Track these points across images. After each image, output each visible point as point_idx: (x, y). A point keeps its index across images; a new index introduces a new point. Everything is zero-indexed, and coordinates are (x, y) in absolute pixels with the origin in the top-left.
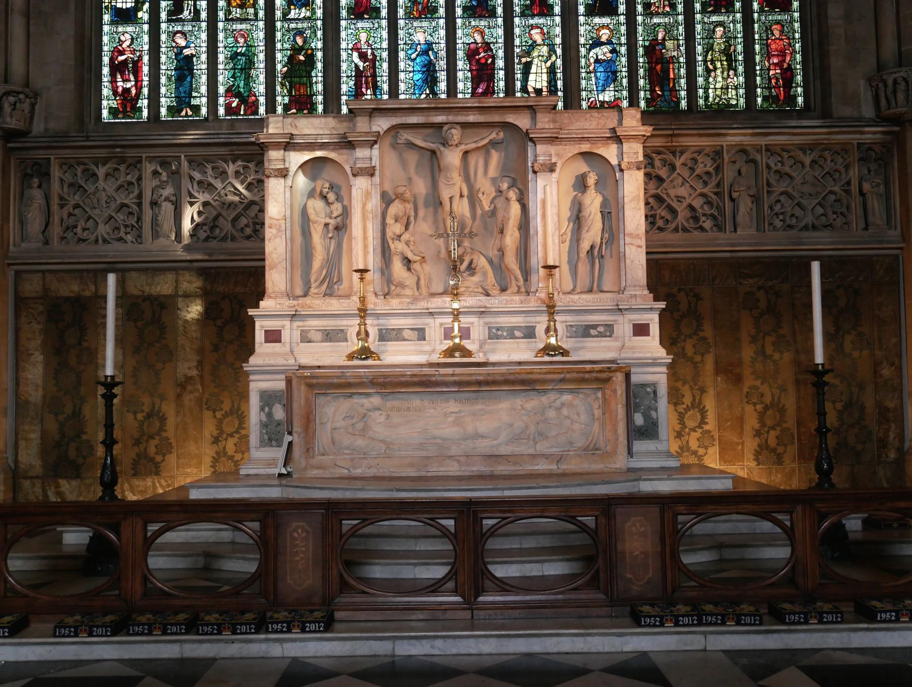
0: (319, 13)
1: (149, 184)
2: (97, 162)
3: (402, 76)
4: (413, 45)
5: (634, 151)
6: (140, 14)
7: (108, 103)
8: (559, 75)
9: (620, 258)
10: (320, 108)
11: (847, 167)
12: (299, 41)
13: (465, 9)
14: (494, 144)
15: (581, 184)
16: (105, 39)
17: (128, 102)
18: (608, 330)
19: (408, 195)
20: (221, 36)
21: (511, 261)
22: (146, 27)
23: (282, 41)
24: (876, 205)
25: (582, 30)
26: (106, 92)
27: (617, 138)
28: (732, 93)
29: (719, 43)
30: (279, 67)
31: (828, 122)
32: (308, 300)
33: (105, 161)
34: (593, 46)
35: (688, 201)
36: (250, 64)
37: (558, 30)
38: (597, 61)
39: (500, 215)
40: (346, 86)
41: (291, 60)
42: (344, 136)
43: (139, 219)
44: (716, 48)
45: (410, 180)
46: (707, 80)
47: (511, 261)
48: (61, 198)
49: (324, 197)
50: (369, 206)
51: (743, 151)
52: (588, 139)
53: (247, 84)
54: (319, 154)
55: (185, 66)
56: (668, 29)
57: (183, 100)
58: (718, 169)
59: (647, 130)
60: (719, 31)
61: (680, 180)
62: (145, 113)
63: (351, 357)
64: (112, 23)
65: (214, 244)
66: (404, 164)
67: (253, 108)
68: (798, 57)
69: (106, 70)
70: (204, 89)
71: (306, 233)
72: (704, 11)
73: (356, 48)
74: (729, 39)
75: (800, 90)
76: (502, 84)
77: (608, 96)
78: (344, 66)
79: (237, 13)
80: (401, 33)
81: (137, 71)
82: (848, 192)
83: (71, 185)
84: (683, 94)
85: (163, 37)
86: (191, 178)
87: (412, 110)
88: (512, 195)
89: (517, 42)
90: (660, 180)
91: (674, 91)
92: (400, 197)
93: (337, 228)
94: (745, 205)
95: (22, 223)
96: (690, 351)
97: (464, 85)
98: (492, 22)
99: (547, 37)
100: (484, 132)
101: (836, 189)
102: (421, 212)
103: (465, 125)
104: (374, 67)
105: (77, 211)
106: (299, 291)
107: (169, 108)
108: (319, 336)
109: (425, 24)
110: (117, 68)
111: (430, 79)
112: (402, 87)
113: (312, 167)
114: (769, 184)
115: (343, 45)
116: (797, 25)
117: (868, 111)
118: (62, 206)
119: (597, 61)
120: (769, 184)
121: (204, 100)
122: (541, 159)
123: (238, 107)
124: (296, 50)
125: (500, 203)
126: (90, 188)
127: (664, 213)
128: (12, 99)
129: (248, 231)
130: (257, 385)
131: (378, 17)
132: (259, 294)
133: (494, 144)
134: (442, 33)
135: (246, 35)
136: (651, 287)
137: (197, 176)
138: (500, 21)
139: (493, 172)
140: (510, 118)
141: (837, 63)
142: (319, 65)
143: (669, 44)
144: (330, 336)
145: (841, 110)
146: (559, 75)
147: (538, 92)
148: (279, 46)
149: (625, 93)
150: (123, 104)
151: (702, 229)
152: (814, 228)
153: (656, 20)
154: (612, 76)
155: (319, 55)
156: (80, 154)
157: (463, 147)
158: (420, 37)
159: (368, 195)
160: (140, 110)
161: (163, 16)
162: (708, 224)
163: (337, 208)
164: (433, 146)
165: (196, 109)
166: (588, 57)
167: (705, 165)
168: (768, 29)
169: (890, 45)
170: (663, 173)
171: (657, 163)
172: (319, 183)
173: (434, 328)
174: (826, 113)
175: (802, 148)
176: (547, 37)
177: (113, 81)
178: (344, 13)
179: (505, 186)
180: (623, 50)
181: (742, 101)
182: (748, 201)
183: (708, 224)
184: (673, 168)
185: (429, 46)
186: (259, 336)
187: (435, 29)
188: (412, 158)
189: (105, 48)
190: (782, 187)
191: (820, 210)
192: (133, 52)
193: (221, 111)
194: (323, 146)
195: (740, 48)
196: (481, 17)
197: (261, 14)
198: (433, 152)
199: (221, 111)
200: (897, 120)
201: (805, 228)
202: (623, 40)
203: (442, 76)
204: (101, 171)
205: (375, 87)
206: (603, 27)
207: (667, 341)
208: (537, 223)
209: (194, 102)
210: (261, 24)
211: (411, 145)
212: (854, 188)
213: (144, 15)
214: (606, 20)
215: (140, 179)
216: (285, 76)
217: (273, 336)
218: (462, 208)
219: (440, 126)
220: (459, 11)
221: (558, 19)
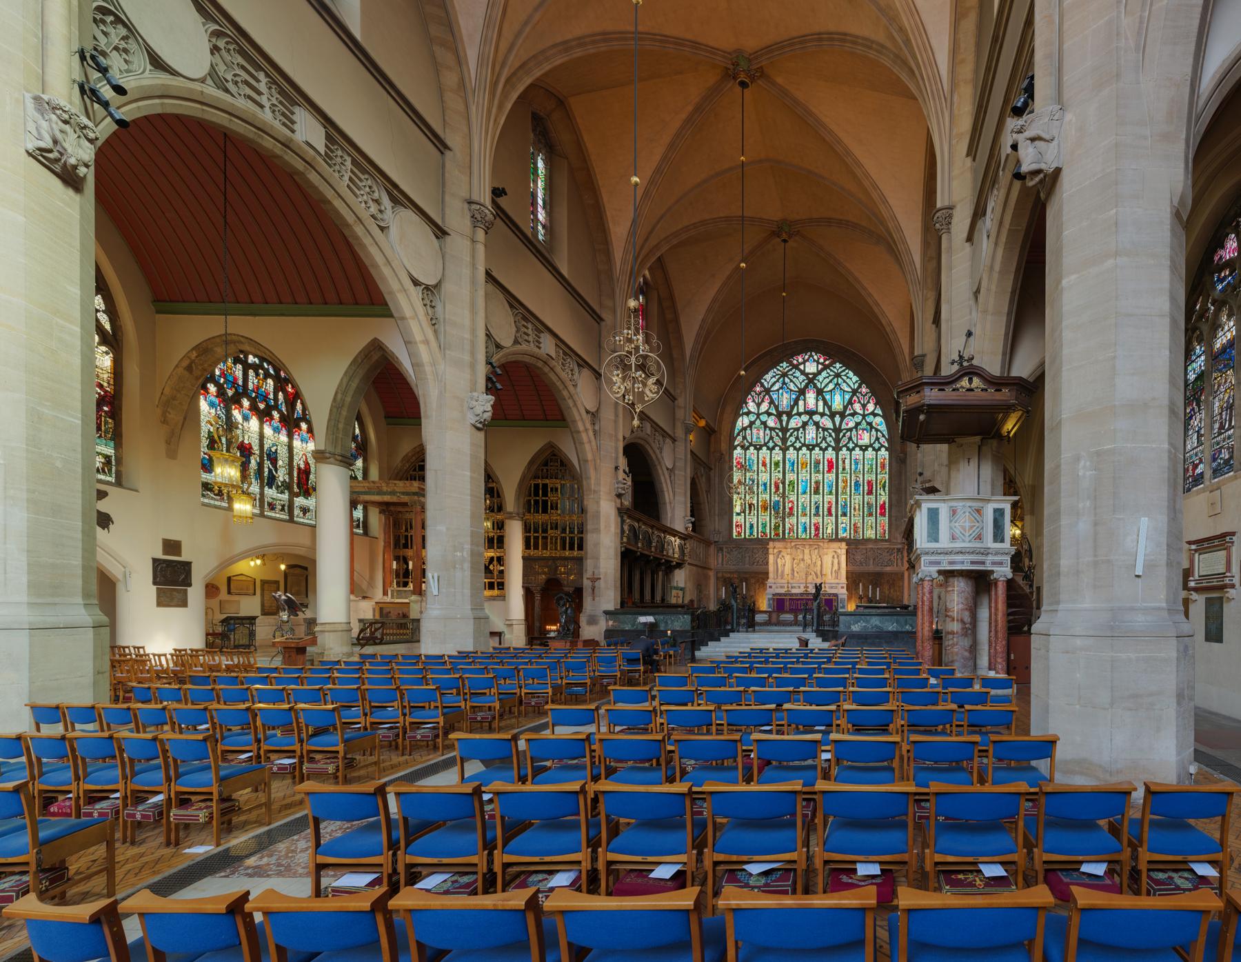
5: (844, 551)
7: (735, 534)
15: (833, 557)
17: (739, 534)
18: (836, 588)
21: (819, 574)
26: (734, 531)
29: (870, 524)
36: (766, 526)
40: (787, 531)
47: (819, 574)
55: (752, 526)
57: (751, 534)
77: (845, 535)
94: (872, 561)
97: (813, 532)
110: (737, 526)
132: (768, 578)
144: (782, 587)
158: (803, 521)
166: (840, 526)
173: (802, 586)
208: (824, 566)
218: (809, 561)
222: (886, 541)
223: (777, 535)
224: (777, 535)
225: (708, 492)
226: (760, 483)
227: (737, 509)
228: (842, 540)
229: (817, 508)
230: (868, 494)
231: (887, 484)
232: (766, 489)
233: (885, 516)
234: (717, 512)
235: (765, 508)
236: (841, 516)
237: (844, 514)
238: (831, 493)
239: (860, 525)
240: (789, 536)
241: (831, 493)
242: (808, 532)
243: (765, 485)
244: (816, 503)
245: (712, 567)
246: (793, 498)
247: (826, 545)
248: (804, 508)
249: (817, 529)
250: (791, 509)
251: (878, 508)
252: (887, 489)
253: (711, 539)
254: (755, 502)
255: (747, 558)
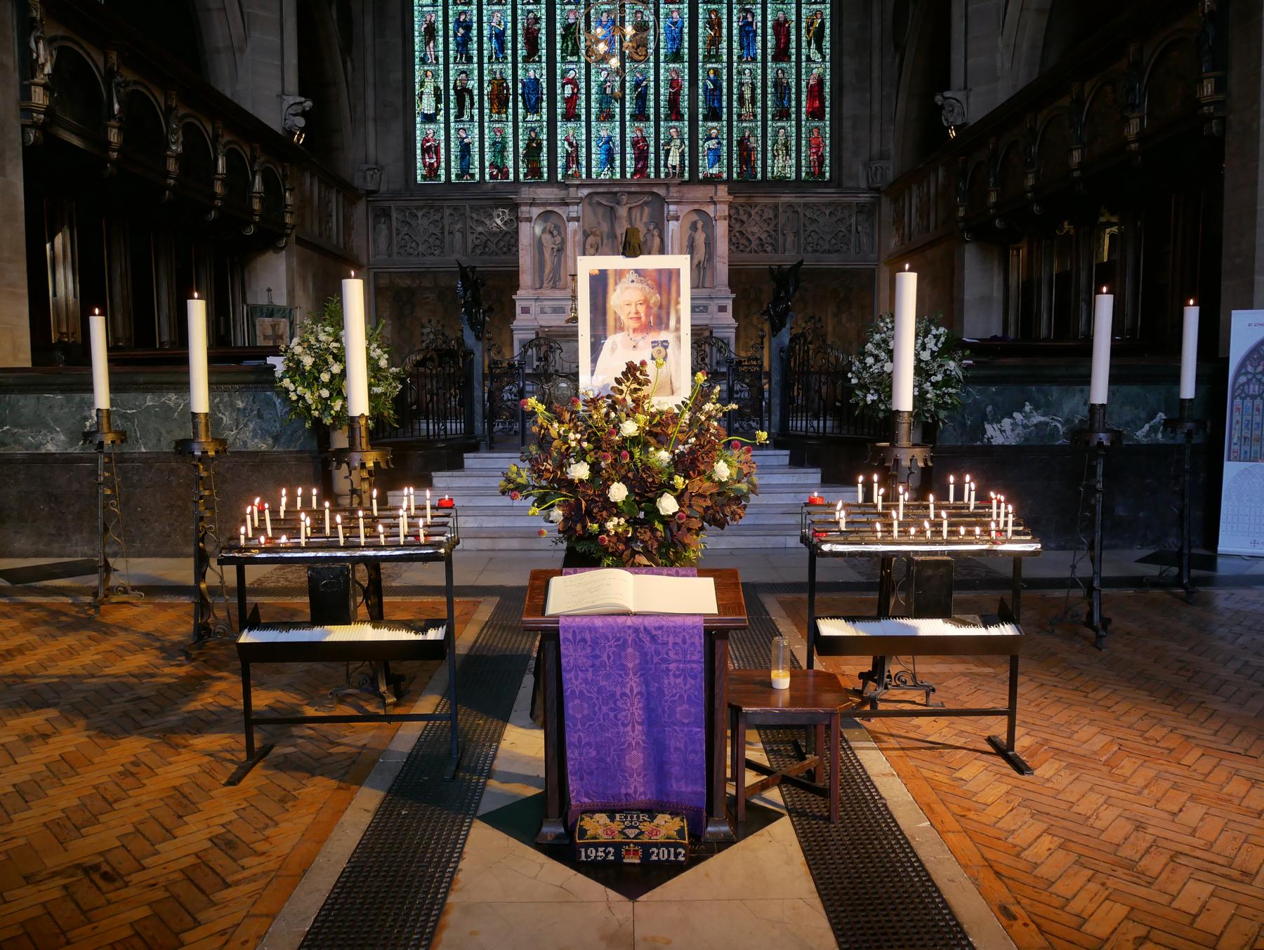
0: (545, 117)
1: (446, 221)
2: (418, 208)
3: (593, 156)
4: (600, 138)
5: (723, 209)
6: (438, 117)
7: (420, 172)
8: (687, 157)
9: (714, 269)
10: (546, 175)
11: (850, 216)
12: (533, 135)
13: (632, 116)
14: (646, 203)
15: (694, 227)
16: (418, 132)
17: (432, 171)
19: (598, 233)
20: (486, 131)
22: (442, 125)
23: (523, 134)
24: (864, 239)
25: (700, 129)
26: (419, 165)
27: (715, 203)
28: (788, 170)
29: (781, 139)
30: (521, 150)
31: (840, 190)
32: (543, 291)
33: (422, 208)
34: (707, 140)
35: (758, 235)
36: (504, 148)
37: (686, 130)
38: (709, 149)
39: (649, 243)
40: (560, 162)
41: (528, 147)
42: (563, 199)
43: (442, 242)
44: (780, 142)
45: (599, 223)
46: (773, 161)
48: (397, 229)
49: (551, 233)
50: (577, 238)
51: (790, 205)
52: (697, 202)
53: (502, 161)
54: (549, 208)
55: (465, 149)
56: (752, 130)
57: (465, 170)
58: (776, 216)
59: (731, 198)
60: (782, 131)
61: (753, 223)
62: (443, 178)
63: (567, 321)
64: (422, 122)
65: (485, 257)
66: (595, 214)
67: (506, 175)
68: (828, 149)
69: (419, 152)
70: (477, 163)
71: (541, 253)
72: (773, 119)
73: (567, 139)
74: (787, 137)
75: (827, 169)
76: (653, 162)
77: (715, 171)
78: (559, 150)
79: (495, 117)
80: (593, 131)
81: (437, 153)
82: (850, 231)
83: (403, 222)
84: (759, 170)
85: (452, 132)
86: (472, 218)
87: (600, 185)
88: (656, 233)
89: (662, 136)
90: (743, 222)
91: (754, 168)
92: (593, 233)
93: (558, 250)
94: (790, 238)
95: (375, 241)
96: (755, 321)
98: (647, 124)
99: (680, 134)
100: (640, 197)
101: (843, 229)
102: (605, 241)
103: (630, 193)
104: (577, 151)
105: (406, 237)
106: (537, 286)
107: (457, 175)
108: (549, 310)
109: (608, 125)
110: (425, 151)
111: (610, 159)
112: (594, 163)
113: (545, 216)
114: (804, 225)
115: (559, 137)
116: (828, 129)
117: (863, 184)
118: (398, 234)
119: (709, 149)
120: (804, 225)
121: (477, 170)
122: (671, 213)
123: (497, 174)
124: (531, 140)
125: (649, 236)
126: (413, 223)
127: (744, 242)
128: (371, 172)
129: (505, 249)
130: (518, 336)
131: (580, 120)
132: (516, 287)
133: (646, 203)
134: (618, 130)
135: (501, 131)
136: (731, 285)
137: (474, 216)
138: (652, 123)
139: (645, 219)
140: (655, 190)
141: (846, 155)
142: (545, 150)
143: (752, 139)
145: (847, 183)
146: (687, 157)
147: (674, 167)
148: (521, 137)
149: (725, 169)
150: (429, 172)
151: (766, 252)
152: (829, 252)
153: (744, 125)
154: (718, 158)
155: (545, 143)
156: (408, 204)
157: (629, 206)
158: (603, 133)
159: (575, 232)
160: (439, 176)
161: (452, 118)
162: (769, 249)
163: (558, 239)
164: (612, 205)
165: (472, 176)
166: (704, 146)
167: (769, 214)
168: (810, 131)
169: (876, 147)
170: (744, 218)
171: (741, 212)
172: (549, 224)
174: (840, 185)
175: (824, 204)
176: (680, 134)
177: (423, 159)
178: (559, 118)
179: (652, 227)
180: (725, 142)
181: (794, 175)
182: (793, 235)
183: (769, 249)
184: (750, 215)
185: (610, 139)
186: (518, 310)
187: (614, 128)
188: (600, 211)
189: (418, 138)
190: (810, 228)
191: (833, 241)
192: (435, 140)
193: (487, 177)
194: (551, 204)
195: (793, 142)
196: (641, 121)
197: (510, 118)
198: (612, 208)
199: (487, 177)
200: (878, 190)
201: (823, 252)
202: (725, 136)
203: (617, 157)
204: (420, 214)
205: (578, 164)
206: (713, 128)
207: (735, 315)
209: (471, 171)
210: (510, 124)
211: (599, 204)
212: (853, 228)
213: (441, 118)
214: (715, 124)
215: (442, 218)
216: (525, 156)
217: (526, 310)
219: (616, 193)
220: (628, 117)
221: (686, 123)
222: (827, 184)
223: (534, 171)
224: (534, 171)
225: (347, 50)
226: (486, 33)
227: (427, 105)
228: (712, 181)
229: (641, 99)
230: (776, 59)
231: (828, 31)
232: (502, 47)
233: (822, 118)
234: (370, 112)
235: (500, 100)
236: (706, 119)
237: (713, 115)
238: (676, 57)
239: (753, 143)
240: (565, 176)
241: (676, 57)
242: (618, 163)
243: (500, 36)
244: (637, 84)
245: (364, 260)
246: (576, 71)
247: (674, 192)
248: (605, 99)
249: (641, 156)
250: (571, 101)
251: (804, 97)
252: (827, 43)
253: (358, 182)
254: (473, 84)
255: (458, 235)
